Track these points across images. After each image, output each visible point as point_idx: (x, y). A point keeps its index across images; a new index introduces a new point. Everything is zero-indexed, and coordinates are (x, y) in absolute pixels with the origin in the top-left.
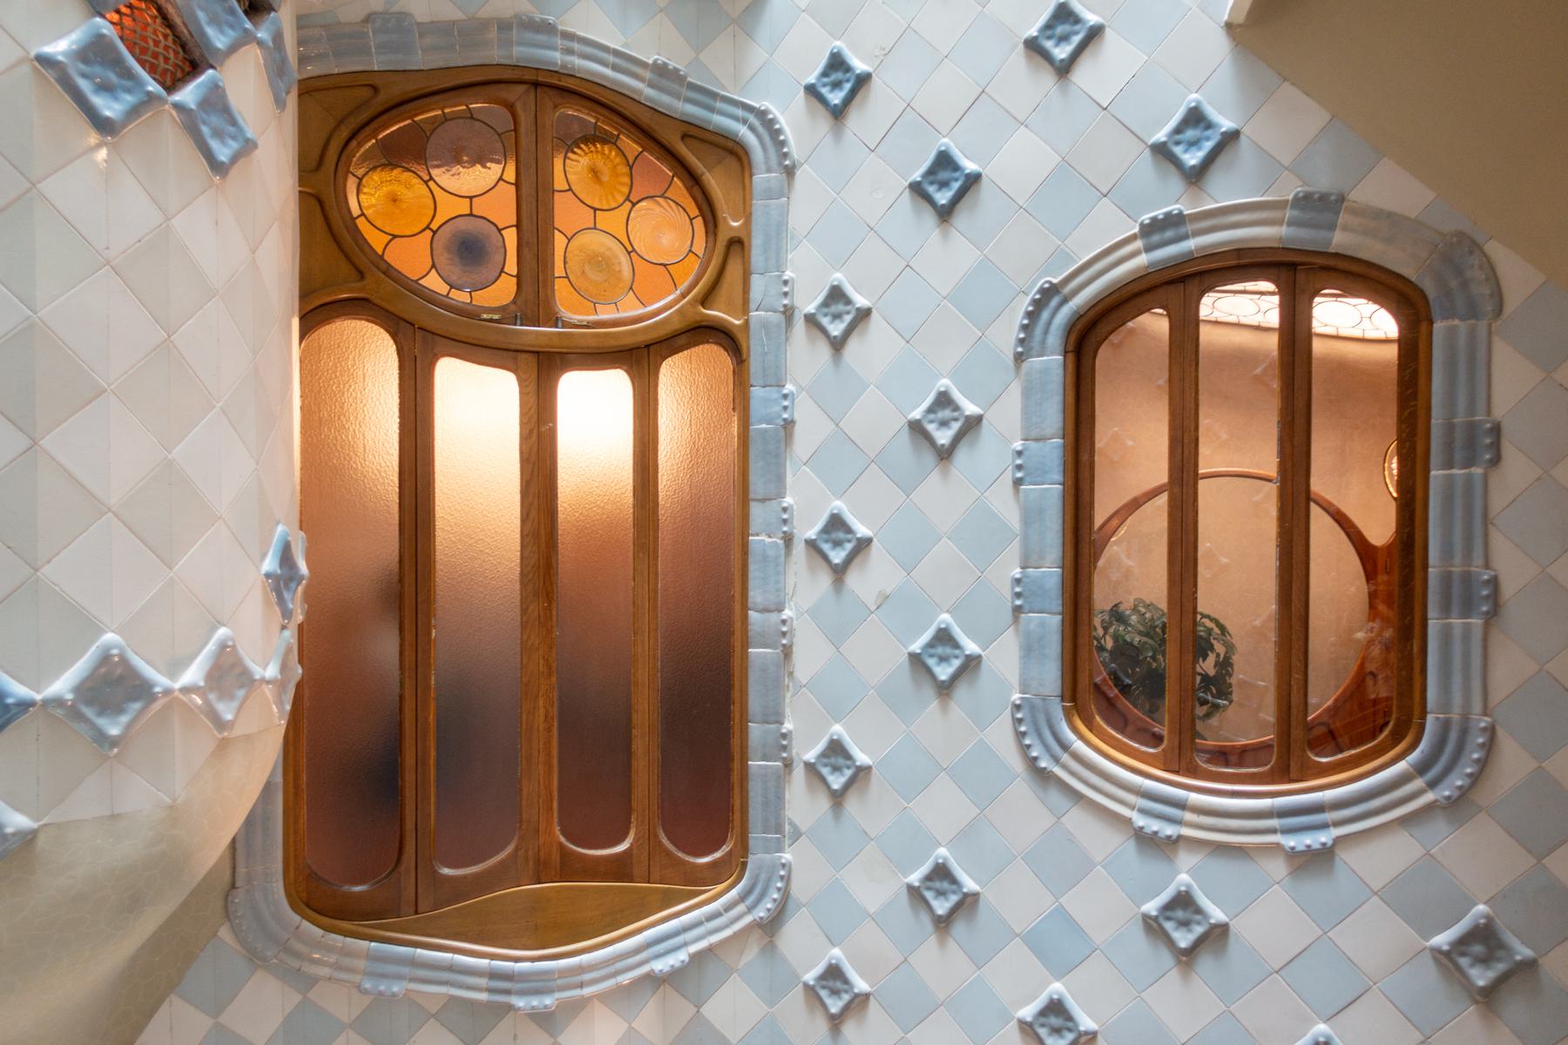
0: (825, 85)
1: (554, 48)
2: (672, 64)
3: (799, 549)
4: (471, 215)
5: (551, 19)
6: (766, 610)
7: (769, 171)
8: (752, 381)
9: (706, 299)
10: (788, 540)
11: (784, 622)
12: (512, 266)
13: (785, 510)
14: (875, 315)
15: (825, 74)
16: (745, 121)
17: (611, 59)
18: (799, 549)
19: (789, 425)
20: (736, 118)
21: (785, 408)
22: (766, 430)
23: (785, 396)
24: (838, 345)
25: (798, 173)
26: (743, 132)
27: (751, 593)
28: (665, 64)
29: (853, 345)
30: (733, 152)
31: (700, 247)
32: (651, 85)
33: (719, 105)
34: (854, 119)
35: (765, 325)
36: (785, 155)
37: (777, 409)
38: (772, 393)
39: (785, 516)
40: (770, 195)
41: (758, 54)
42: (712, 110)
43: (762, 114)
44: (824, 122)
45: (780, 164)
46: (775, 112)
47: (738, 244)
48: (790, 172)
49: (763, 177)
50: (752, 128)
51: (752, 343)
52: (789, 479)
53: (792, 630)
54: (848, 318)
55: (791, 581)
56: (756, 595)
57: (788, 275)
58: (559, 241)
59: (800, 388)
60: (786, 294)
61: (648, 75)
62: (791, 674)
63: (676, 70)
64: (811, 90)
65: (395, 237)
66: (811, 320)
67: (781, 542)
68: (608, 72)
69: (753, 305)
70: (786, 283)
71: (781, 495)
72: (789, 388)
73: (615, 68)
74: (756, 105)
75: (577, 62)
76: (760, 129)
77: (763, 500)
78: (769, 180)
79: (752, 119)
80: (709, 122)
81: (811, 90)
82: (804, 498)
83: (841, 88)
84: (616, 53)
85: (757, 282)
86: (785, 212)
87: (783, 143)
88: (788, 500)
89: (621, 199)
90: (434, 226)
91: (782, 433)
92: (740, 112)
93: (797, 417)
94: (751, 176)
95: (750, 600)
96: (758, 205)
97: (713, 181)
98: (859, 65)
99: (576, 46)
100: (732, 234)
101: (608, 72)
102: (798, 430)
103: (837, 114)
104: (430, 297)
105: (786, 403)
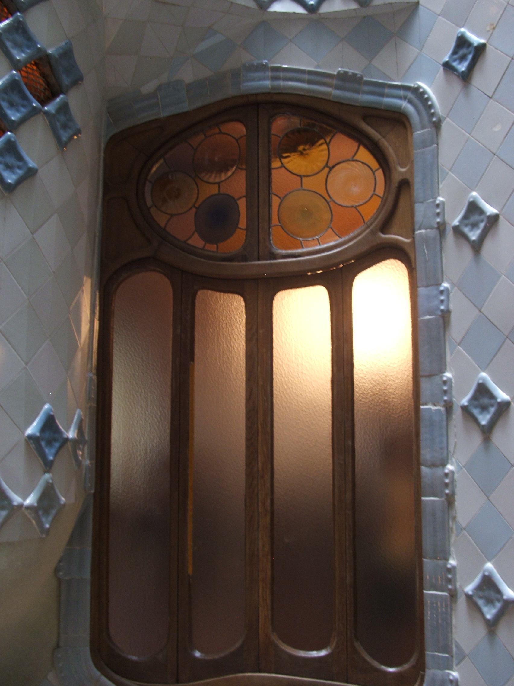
0: (455, 60)
1: (264, 79)
2: (351, 71)
3: (457, 414)
4: (219, 194)
5: (265, 62)
6: (433, 465)
7: (423, 128)
8: (419, 285)
9: (385, 227)
10: (449, 407)
11: (446, 475)
12: (243, 223)
13: (445, 383)
14: (501, 218)
15: (455, 52)
16: (405, 98)
17: (306, 77)
18: (457, 414)
19: (446, 316)
20: (399, 97)
21: (442, 301)
22: (429, 320)
23: (442, 292)
24: (477, 247)
25: (444, 126)
26: (404, 104)
27: (422, 452)
28: (346, 73)
29: (488, 245)
30: (398, 120)
31: (380, 191)
32: (337, 88)
33: (387, 91)
34: (478, 80)
35: (426, 239)
36: (433, 115)
37: (436, 302)
38: (432, 291)
39: (445, 388)
40: (425, 145)
41: (411, 51)
42: (382, 95)
43: (416, 90)
44: (457, 85)
45: (430, 121)
46: (424, 86)
47: (405, 185)
48: (437, 126)
49: (419, 133)
50: (410, 102)
51: (418, 254)
52: (448, 358)
53: (453, 481)
54: (482, 225)
55: (452, 440)
56: (426, 454)
57: (440, 199)
58: (275, 201)
59: (453, 285)
60: (438, 214)
61: (335, 82)
62: (454, 518)
63: (354, 75)
64: (447, 66)
65: (172, 216)
66: (457, 230)
67: (442, 409)
68: (305, 86)
69: (417, 227)
70: (438, 206)
71: (442, 371)
72: (445, 285)
73: (309, 82)
74: (412, 85)
75: (282, 83)
76: (416, 101)
77: (430, 376)
78: (423, 134)
79: (410, 95)
80: (381, 104)
81: (447, 66)
82: (460, 376)
83: (467, 58)
84: (310, 73)
85: (420, 209)
86: (436, 155)
87: (431, 107)
88: (448, 375)
89: (322, 165)
90: (197, 205)
91: (441, 321)
92: (402, 93)
93: (451, 307)
94: (412, 133)
95: (422, 457)
96: (417, 152)
97: (385, 143)
98: (476, 39)
99: (281, 74)
100: (401, 178)
101: (305, 86)
102: (454, 317)
103: (466, 78)
104: (191, 251)
105: (442, 298)
